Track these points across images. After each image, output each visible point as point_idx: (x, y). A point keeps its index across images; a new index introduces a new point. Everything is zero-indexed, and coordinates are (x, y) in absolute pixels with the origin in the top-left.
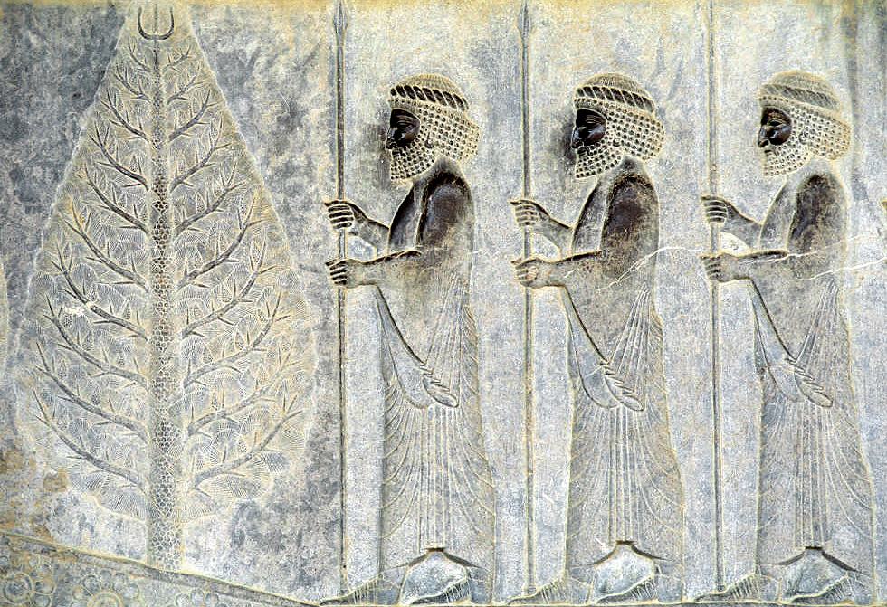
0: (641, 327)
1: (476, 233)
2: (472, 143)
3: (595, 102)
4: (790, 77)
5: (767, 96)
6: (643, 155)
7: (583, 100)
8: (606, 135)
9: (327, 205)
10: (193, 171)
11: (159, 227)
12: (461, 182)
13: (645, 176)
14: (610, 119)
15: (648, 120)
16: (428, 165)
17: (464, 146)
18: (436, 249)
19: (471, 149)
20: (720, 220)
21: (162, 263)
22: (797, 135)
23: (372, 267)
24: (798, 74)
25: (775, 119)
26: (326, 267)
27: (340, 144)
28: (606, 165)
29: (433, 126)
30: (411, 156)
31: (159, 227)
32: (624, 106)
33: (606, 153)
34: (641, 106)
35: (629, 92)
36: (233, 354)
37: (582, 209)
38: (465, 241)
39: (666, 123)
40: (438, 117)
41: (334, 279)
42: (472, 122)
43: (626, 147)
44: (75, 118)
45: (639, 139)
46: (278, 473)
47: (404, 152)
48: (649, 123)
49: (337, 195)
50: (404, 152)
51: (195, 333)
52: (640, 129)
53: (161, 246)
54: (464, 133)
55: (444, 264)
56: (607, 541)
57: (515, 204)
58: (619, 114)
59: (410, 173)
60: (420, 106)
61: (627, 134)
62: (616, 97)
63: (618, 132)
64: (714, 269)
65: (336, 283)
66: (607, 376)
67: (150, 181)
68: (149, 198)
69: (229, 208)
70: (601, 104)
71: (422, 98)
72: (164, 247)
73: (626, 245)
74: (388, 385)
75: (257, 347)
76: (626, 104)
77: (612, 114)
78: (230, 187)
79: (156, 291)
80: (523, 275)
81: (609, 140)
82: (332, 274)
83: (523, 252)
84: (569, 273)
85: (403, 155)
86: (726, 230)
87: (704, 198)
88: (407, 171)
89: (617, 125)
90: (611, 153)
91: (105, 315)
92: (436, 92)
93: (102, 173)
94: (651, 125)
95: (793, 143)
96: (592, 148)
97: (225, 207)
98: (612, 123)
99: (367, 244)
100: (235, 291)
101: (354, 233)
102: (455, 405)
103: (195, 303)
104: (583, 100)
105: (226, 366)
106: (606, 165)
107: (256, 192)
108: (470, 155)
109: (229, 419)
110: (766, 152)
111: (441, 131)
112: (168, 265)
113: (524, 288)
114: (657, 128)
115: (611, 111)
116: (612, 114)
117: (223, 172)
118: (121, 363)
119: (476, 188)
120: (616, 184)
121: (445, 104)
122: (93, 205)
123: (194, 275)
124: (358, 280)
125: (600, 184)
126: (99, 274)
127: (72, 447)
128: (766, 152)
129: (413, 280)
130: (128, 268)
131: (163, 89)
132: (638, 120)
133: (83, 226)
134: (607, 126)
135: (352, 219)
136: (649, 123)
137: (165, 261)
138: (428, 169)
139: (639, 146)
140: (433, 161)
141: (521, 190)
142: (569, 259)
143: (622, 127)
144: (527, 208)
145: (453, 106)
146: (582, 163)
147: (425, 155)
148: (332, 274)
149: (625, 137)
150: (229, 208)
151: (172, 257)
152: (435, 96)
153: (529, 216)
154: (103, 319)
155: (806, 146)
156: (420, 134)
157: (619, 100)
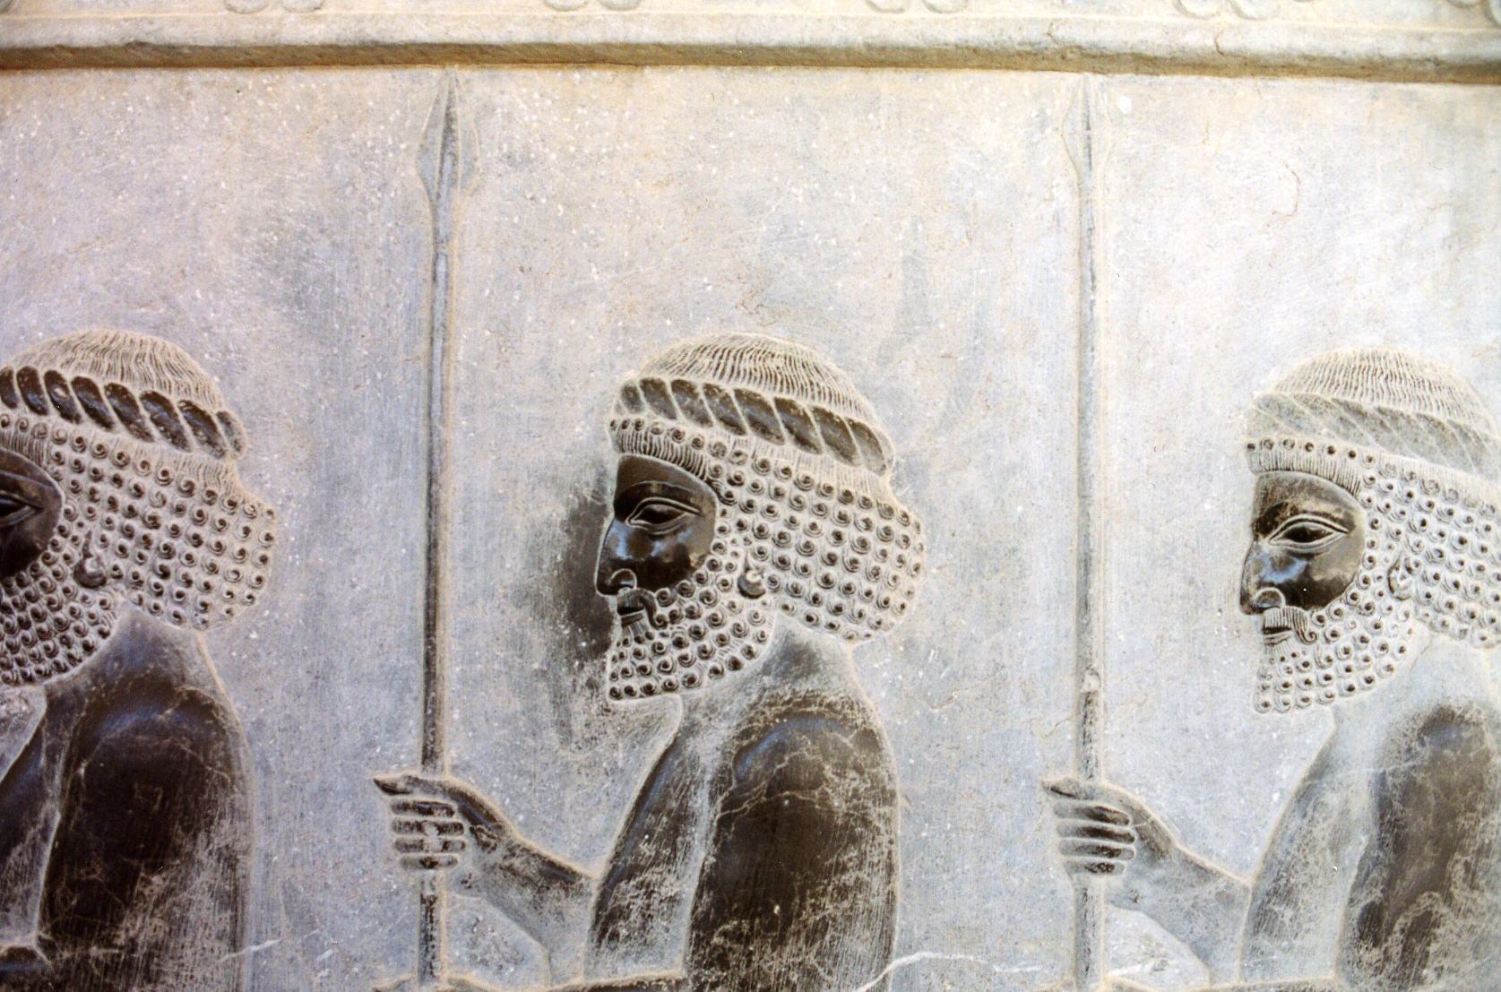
1: (255, 882)
3: (677, 435)
4: (1350, 370)
6: (850, 627)
7: (638, 425)
8: (716, 556)
12: (201, 709)
14: (728, 499)
17: (213, 580)
19: (242, 590)
20: (1108, 869)
22: (1380, 570)
24: (1375, 357)
28: (711, 664)
29: (102, 512)
32: (784, 453)
34: (846, 454)
35: (804, 404)
39: (931, 511)
40: (117, 481)
43: (790, 601)
45: (834, 572)
48: (872, 515)
52: (838, 536)
57: (389, 789)
58: (763, 481)
61: (791, 554)
62: (754, 423)
63: (756, 544)
70: (697, 443)
76: (789, 445)
77: (736, 481)
87: (1055, 790)
90: (731, 621)
92: (117, 391)
94: (879, 523)
95: (1365, 597)
98: (735, 514)
104: (638, 425)
106: (711, 664)
108: (239, 610)
110: (1268, 630)
111: (128, 532)
115: (735, 471)
116: (736, 481)
119: (259, 724)
120: (746, 734)
121: (145, 435)
125: (690, 730)
128: (1268, 630)
132: (831, 503)
134: (719, 523)
136: (872, 515)
139: (833, 597)
141: (413, 741)
143: (774, 527)
144: (425, 810)
145: (177, 439)
146: (628, 651)
149: (783, 563)
152: (108, 405)
153: (432, 838)
155: (1408, 605)
157: (764, 430)
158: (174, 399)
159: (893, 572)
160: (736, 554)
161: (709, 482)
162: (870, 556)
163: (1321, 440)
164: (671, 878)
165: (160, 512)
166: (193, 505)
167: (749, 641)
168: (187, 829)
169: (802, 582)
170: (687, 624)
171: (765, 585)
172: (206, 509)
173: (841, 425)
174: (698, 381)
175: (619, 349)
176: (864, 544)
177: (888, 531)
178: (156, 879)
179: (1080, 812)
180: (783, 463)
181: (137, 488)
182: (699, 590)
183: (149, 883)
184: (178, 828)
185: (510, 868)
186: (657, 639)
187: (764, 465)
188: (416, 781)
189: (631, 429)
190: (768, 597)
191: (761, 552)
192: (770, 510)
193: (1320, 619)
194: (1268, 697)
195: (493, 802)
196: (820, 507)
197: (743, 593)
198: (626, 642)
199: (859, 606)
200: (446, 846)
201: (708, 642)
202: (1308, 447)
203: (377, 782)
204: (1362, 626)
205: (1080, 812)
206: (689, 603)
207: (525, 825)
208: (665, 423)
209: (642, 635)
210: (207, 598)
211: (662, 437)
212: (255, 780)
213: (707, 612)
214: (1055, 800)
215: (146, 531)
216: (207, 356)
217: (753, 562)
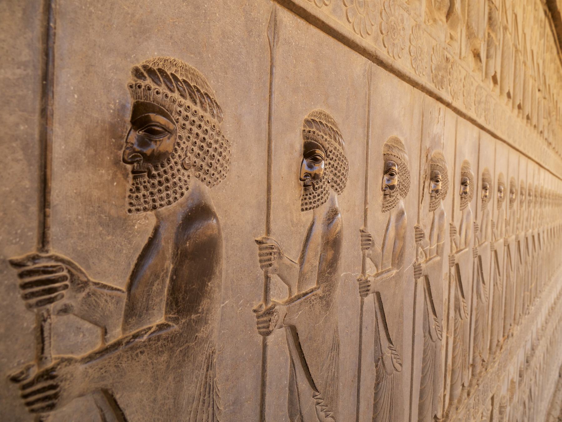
5: (389, 153)
18: (193, 316)
29: (193, 139)
40: (200, 126)
47: (154, 172)
57: (259, 242)
59: (157, 204)
64: (365, 289)
80: (265, 325)
83: (262, 298)
85: (153, 177)
88: (154, 201)
89: (332, 162)
99: (87, 325)
101: (65, 310)
104: (314, 132)
111: (201, 148)
115: (330, 149)
120: (329, 219)
135: (66, 287)
138: (180, 200)
140: (187, 189)
143: (335, 165)
183: (208, 285)
186: (315, 194)
189: (312, 133)
198: (307, 195)
203: (257, 241)
206: (321, 184)
214: (360, 234)
215: (208, 149)
216: (212, 82)
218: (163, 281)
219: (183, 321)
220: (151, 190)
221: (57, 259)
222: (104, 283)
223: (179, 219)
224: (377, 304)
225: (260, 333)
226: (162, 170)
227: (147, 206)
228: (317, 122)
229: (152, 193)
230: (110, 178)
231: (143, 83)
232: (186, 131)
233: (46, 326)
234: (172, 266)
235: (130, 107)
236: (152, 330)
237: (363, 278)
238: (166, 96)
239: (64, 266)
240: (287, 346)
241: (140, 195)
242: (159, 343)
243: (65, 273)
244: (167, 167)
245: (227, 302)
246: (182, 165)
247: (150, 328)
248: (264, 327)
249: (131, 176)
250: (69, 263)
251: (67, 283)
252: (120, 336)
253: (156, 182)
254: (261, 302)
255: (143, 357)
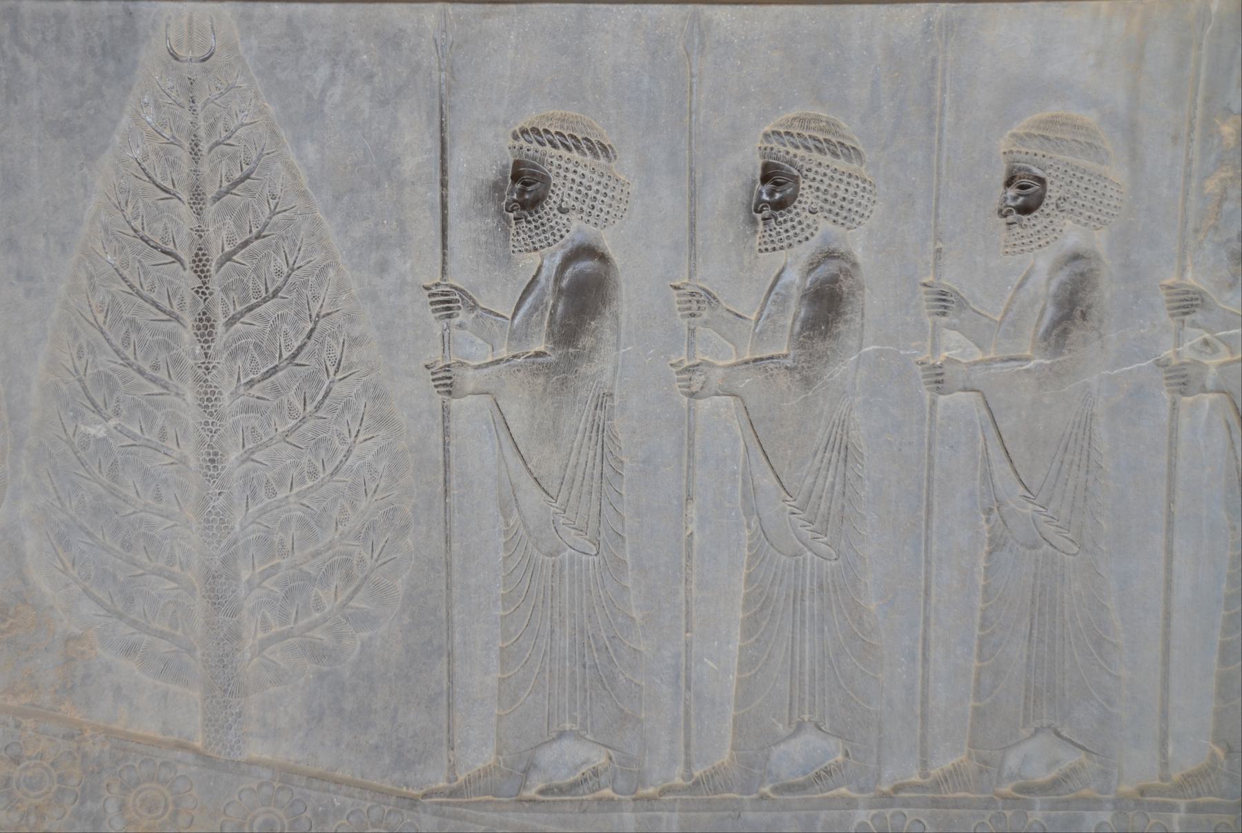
0: (839, 453)
1: (623, 325)
2: (621, 205)
3: (788, 153)
5: (1014, 149)
6: (848, 224)
7: (772, 149)
9: (427, 288)
10: (245, 244)
11: (201, 320)
12: (603, 258)
13: (850, 253)
14: (806, 177)
15: (857, 178)
16: (562, 237)
17: (610, 210)
18: (571, 350)
19: (619, 214)
20: (944, 314)
21: (207, 369)
22: (1053, 200)
23: (485, 371)
24: (1057, 116)
25: (1025, 182)
26: (426, 370)
27: (444, 206)
28: (797, 239)
29: (569, 184)
30: (538, 224)
31: (201, 320)
32: (827, 159)
33: (800, 223)
34: (849, 158)
35: (834, 140)
36: (305, 487)
37: (765, 293)
38: (608, 335)
40: (575, 172)
41: (436, 386)
42: (623, 177)
43: (827, 214)
44: (85, 170)
45: (844, 204)
46: (365, 635)
47: (530, 218)
48: (859, 182)
49: (439, 276)
50: (530, 218)
51: (253, 460)
52: (847, 190)
53: (206, 346)
54: (610, 194)
55: (582, 370)
56: (787, 721)
57: (676, 288)
59: (537, 246)
60: (555, 160)
61: (829, 197)
63: (816, 194)
65: (438, 392)
66: (792, 516)
67: (187, 258)
68: (188, 280)
69: (294, 294)
70: (795, 156)
71: (555, 146)
72: (209, 347)
73: (820, 346)
74: (508, 525)
75: (335, 478)
76: (829, 156)
77: (809, 170)
78: (296, 266)
79: (200, 405)
81: (803, 205)
82: (433, 380)
83: (685, 353)
84: (747, 381)
85: (529, 222)
86: (952, 327)
87: (925, 285)
88: (533, 243)
89: (815, 184)
91: (134, 437)
92: (572, 137)
93: (123, 248)
95: (1047, 211)
96: (782, 215)
97: (290, 292)
98: (808, 183)
99: (479, 341)
100: (305, 405)
101: (460, 326)
102: (596, 552)
103: (253, 420)
104: (772, 149)
105: (295, 503)
106: (797, 239)
107: (332, 273)
108: (617, 221)
109: (301, 570)
111: (579, 192)
112: (214, 372)
113: (686, 399)
114: (868, 188)
115: (808, 166)
116: (809, 170)
117: (286, 245)
118: (158, 498)
120: (812, 264)
122: (112, 289)
123: (251, 383)
124: (470, 386)
126: (124, 383)
127: (99, 602)
128: (1009, 224)
129: (541, 389)
130: (162, 374)
131: (202, 133)
132: (845, 178)
133: (101, 318)
135: (459, 308)
137: (211, 366)
138: (561, 242)
139: (844, 213)
142: (747, 363)
143: (823, 187)
144: (692, 294)
145: (596, 155)
146: (766, 234)
147: (557, 223)
148: (433, 380)
149: (826, 200)
150: (294, 294)
151: (221, 361)
153: (695, 306)
154: (132, 442)
155: (1064, 214)
156: (551, 194)
157: (820, 150)
158: (593, 140)
159: (866, 203)
160: (808, 198)
161: (799, 171)
162: (858, 198)
163: (1032, 151)
164: (782, 318)
165: (591, 184)
166: (604, 180)
167: (812, 230)
168: (603, 304)
169: (832, 208)
170: (790, 224)
171: (818, 210)
172: (608, 182)
173: (847, 148)
174: (794, 131)
175: (762, 118)
176: (856, 193)
177: (864, 188)
178: (592, 323)
179: (933, 293)
180: (827, 163)
181: (583, 175)
182: (795, 211)
184: (600, 304)
185: (722, 316)
186: (778, 230)
187: (820, 164)
188: (688, 284)
189: (768, 150)
190: (819, 214)
191: (818, 197)
192: (822, 181)
193: (1029, 219)
194: (1008, 250)
195: (715, 294)
196: (840, 180)
197: (810, 212)
198: (765, 231)
199: (853, 216)
200: (699, 309)
201: (797, 231)
202: (1027, 153)
203: (671, 286)
204: (1046, 221)
205: (933, 293)
206: (790, 216)
207: (726, 301)
208: (783, 149)
209: (772, 228)
210: (607, 217)
211: (782, 154)
212: (624, 286)
213: (797, 219)
217: (814, 200)
218: (543, 314)
219: (560, 352)
220: (529, 233)
221: (452, 287)
222: (492, 309)
223: (558, 260)
224: (985, 412)
225: (682, 392)
226: (537, 216)
227: (527, 247)
228: (779, 134)
229: (529, 236)
230: (495, 225)
231: (517, 144)
232: (560, 178)
233: (446, 334)
234: (551, 302)
235: (511, 165)
236: (528, 355)
237: (931, 362)
238: (536, 151)
239: (456, 292)
240: (736, 422)
241: (520, 238)
242: (535, 366)
243: (457, 297)
244: (542, 213)
245: (629, 348)
246: (558, 209)
247: (528, 353)
248: (684, 387)
249: (513, 222)
250: (461, 290)
251: (460, 304)
252: (505, 355)
253: (532, 226)
254: (684, 357)
255: (520, 375)
